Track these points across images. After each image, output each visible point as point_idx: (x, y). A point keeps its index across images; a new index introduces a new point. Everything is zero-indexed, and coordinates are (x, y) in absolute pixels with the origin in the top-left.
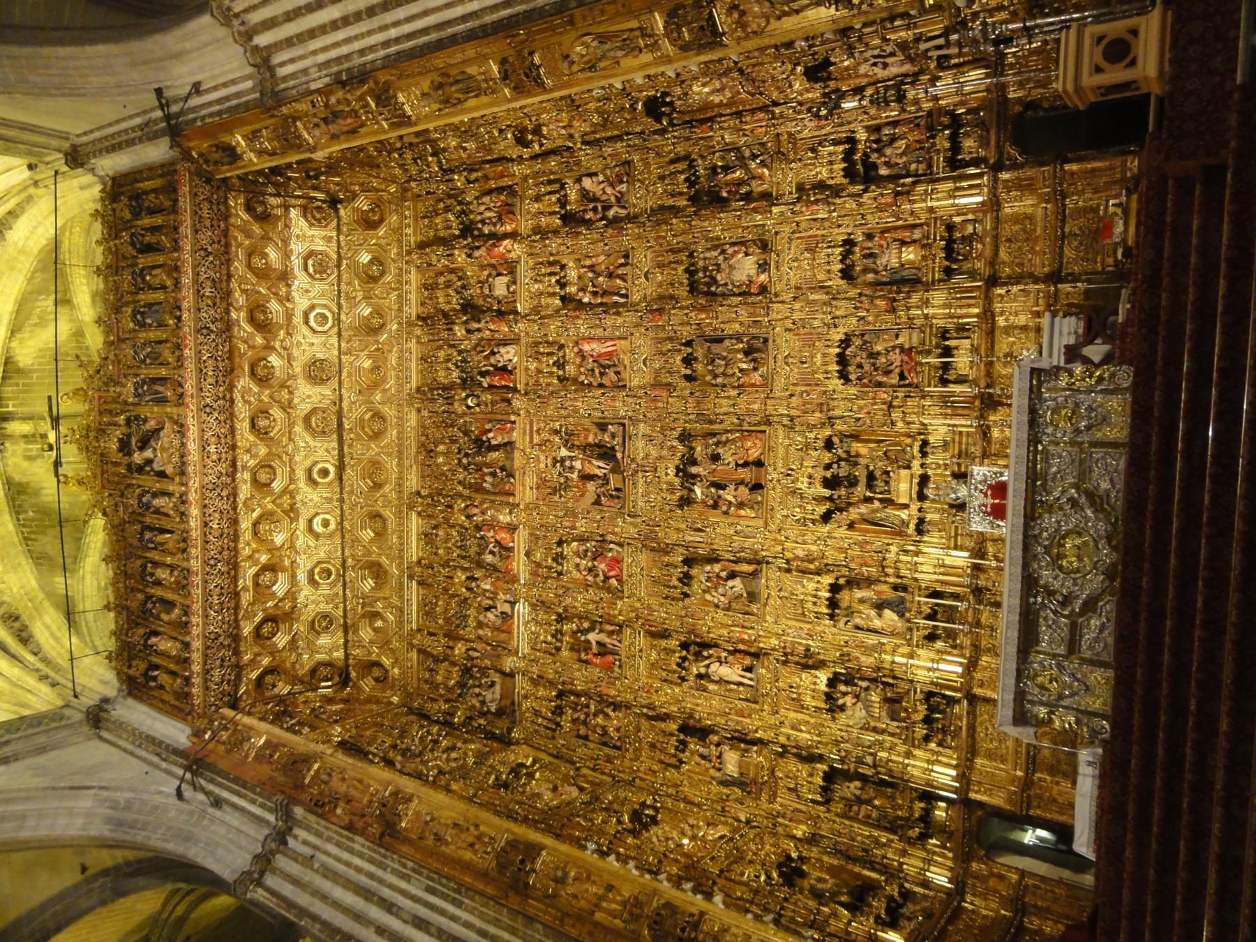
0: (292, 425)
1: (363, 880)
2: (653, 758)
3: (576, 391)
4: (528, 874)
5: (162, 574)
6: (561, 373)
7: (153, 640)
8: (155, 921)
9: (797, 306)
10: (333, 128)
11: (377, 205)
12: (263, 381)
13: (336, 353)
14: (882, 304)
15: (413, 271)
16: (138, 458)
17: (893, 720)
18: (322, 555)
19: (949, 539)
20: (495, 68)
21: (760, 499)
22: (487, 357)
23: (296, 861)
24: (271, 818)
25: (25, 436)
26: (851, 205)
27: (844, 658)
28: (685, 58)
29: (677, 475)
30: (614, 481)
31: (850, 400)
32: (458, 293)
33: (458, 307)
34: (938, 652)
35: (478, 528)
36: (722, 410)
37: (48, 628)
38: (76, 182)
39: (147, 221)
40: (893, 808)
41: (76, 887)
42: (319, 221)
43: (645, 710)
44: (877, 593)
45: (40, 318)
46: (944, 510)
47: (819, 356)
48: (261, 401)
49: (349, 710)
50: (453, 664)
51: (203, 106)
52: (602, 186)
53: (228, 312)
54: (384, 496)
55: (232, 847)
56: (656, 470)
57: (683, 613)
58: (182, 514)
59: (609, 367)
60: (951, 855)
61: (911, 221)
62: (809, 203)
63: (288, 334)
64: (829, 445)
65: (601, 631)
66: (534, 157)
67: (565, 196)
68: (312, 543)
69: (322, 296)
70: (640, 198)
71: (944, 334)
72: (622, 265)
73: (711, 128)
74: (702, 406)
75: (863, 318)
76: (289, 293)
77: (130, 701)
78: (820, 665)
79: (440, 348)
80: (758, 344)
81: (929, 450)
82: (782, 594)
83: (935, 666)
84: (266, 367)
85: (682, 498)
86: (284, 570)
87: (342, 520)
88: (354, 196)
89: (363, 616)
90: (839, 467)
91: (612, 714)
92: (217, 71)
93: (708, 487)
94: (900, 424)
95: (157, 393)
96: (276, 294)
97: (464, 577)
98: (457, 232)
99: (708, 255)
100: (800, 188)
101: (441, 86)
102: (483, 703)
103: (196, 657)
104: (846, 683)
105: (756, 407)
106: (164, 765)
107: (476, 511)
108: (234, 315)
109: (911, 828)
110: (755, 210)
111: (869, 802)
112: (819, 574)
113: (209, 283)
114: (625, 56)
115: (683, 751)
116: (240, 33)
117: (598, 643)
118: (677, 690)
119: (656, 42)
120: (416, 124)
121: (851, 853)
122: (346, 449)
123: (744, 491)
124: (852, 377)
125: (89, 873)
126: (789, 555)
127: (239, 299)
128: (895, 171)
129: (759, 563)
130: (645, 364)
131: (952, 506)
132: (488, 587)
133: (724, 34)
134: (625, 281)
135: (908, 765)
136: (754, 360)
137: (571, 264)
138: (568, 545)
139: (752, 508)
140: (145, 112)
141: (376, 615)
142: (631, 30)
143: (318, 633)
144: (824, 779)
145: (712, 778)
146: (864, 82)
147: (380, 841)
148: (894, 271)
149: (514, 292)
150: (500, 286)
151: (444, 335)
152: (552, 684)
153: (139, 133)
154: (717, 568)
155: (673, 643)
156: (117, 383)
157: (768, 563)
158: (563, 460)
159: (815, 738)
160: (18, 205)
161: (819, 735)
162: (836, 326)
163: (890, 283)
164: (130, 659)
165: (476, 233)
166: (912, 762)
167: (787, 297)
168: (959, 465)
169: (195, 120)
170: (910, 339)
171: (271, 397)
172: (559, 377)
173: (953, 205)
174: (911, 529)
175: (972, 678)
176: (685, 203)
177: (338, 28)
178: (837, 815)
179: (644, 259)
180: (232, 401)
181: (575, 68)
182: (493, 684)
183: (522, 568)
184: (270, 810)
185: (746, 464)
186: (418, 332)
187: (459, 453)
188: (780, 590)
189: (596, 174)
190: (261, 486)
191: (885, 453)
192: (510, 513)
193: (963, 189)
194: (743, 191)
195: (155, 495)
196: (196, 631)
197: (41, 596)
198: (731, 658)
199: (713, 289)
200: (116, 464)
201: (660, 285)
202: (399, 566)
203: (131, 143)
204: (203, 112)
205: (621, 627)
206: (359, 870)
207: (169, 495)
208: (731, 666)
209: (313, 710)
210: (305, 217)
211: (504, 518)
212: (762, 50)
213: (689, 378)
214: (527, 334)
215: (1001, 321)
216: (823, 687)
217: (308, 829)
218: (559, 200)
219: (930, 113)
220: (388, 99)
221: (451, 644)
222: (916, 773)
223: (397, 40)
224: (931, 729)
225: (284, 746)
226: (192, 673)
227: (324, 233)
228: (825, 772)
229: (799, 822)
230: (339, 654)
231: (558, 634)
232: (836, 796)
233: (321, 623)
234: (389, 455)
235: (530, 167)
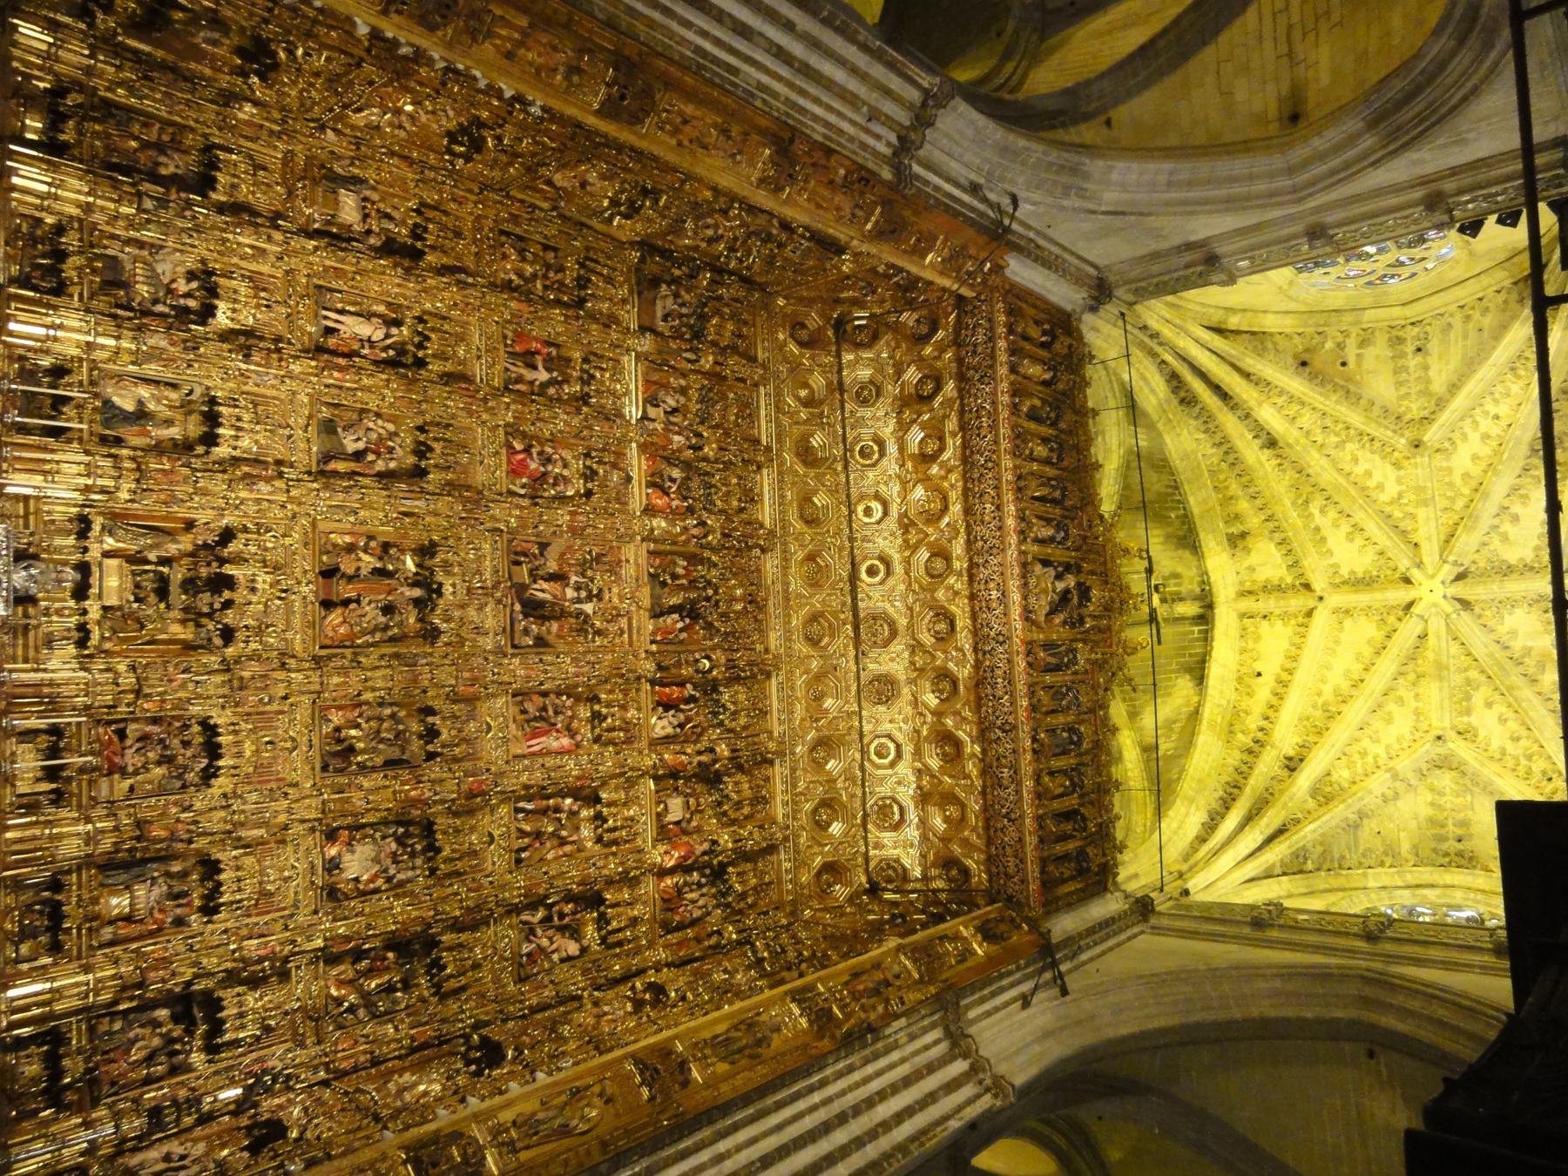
0: (910, 626)
1: (812, 89)
2: (457, 218)
3: (577, 686)
4: (615, 82)
5: (1041, 451)
6: (597, 707)
7: (1047, 376)
8: (1036, 58)
9: (282, 818)
10: (878, 976)
11: (824, 893)
12: (944, 677)
13: (864, 713)
14: (157, 832)
15: (780, 818)
16: (1071, 581)
17: (114, 258)
18: (871, 475)
19: (37, 512)
20: (695, 1074)
21: (325, 558)
22: (689, 720)
23: (887, 116)
24: (916, 168)
25: (1181, 599)
26: (210, 962)
27: (192, 345)
28: (455, 1123)
29: (441, 585)
31: (199, 696)
32: (727, 796)
33: (726, 779)
34: (47, 352)
35: (691, 510)
37: (1152, 391)
38: (1143, 881)
39: (1071, 846)
40: (108, 136)
41: (1117, 102)
42: (889, 867)
43: (470, 280)
44: (146, 434)
45: (1172, 729)
46: (46, 550)
47: (248, 753)
48: (945, 652)
49: (834, 291)
50: (714, 344)
51: (1019, 982)
52: (554, 946)
53: (984, 751)
54: (802, 546)
55: (957, 137)
56: (469, 590)
57: (424, 406)
58: (1023, 519)
59: (536, 719)
60: (15, 64)
61: (118, 950)
62: (272, 957)
63: (917, 732)
64: (228, 635)
65: (532, 383)
66: (641, 972)
67: (599, 929)
68: (883, 489)
69: (882, 779)
70: (503, 937)
71: (58, 798)
72: (524, 850)
73: (413, 1039)
74: (409, 676)
75: (185, 810)
76: (919, 778)
77: (1069, 308)
78: (226, 336)
79: (745, 728)
80: (336, 763)
81: (75, 635)
82: (287, 432)
83: (52, 332)
84: (941, 691)
85: (433, 555)
86: (912, 456)
87: (850, 515)
88: (851, 900)
89: (821, 402)
90: (211, 605)
91: (514, 277)
92: (1006, 1023)
93: (397, 571)
94: (122, 668)
95: (1052, 655)
96: (933, 776)
98: (730, 869)
99: (410, 874)
100: (284, 976)
101: (759, 1043)
102: (676, 295)
103: (1003, 357)
104: (186, 310)
105: (336, 680)
106: (1032, 235)
107: (695, 531)
108: (977, 748)
109: (80, 106)
110: (347, 939)
111: (146, 145)
112: (234, 458)
113: (1005, 782)
114: (534, 1114)
115: (416, 225)
116: (984, 1070)
117: (535, 368)
118: (428, 306)
119: (495, 1138)
120: (786, 993)
121: (171, 76)
122: (849, 601)
123: (347, 566)
124: (196, 728)
125: (1103, 118)
126: (279, 484)
127: (972, 768)
128: (145, 1017)
129: (322, 473)
131: (35, 557)
132: (676, 438)
133: (405, 1162)
134: (519, 830)
135: (88, 194)
136: (339, 741)
137: (589, 844)
138: (577, 492)
139: (335, 545)
140: (1077, 968)
141: (808, 403)
142: (527, 1148)
143: (871, 382)
144: (214, 180)
145: (374, 189)
146: (198, 1132)
147: (795, 133)
148: (141, 879)
149: (658, 803)
150: (676, 809)
151: (740, 744)
152: (593, 317)
153: (1082, 943)
154: (380, 466)
155: (435, 367)
156: (1094, 663)
157: (309, 473)
158: (589, 598)
159: (231, 236)
160: (1197, 851)
161: (225, 241)
162: (225, 795)
163: (145, 861)
164: (1070, 355)
165: (708, 871)
166: (82, 198)
167: (298, 829)
168: (26, 615)
169: (1027, 966)
170: (111, 787)
171: (934, 657)
172: (599, 701)
173: (53, 980)
174: (97, 523)
176: (444, 938)
177: (878, 1093)
178: (192, 130)
179: (496, 860)
180: (976, 650)
181: (597, 1089)
182: (665, 318)
183: (635, 462)
184: (918, 177)
185: (346, 603)
186: (772, 746)
187: (717, 604)
188: (290, 437)
189: (562, 961)
190: (941, 553)
191: (142, 627)
192: (652, 530)
193: (38, 1005)
194: (365, 963)
195: (1052, 539)
196: (1004, 386)
197: (1160, 426)
198: (356, 346)
199: (401, 830)
200: (1092, 573)
201: (473, 829)
202: (782, 464)
203: (1091, 931)
204: (1018, 976)
205: (506, 388)
206: (817, 101)
207: (1037, 541)
208: (355, 337)
209: (874, 292)
210: (905, 869)
211: (660, 524)
212: (349, 1151)
213: (430, 711)
214: (640, 753)
216: (222, 306)
217: (876, 153)
218: (608, 923)
219: (95, 1103)
220: (819, 1018)
221: (718, 368)
222: (75, 183)
223: (811, 1090)
224: (54, 243)
225: (905, 251)
226: (1006, 338)
227: (884, 852)
228: (214, 189)
229: (248, 123)
230: (848, 357)
231: (587, 379)
232: (194, 156)
233: (868, 394)
234: (800, 596)
235: (645, 960)
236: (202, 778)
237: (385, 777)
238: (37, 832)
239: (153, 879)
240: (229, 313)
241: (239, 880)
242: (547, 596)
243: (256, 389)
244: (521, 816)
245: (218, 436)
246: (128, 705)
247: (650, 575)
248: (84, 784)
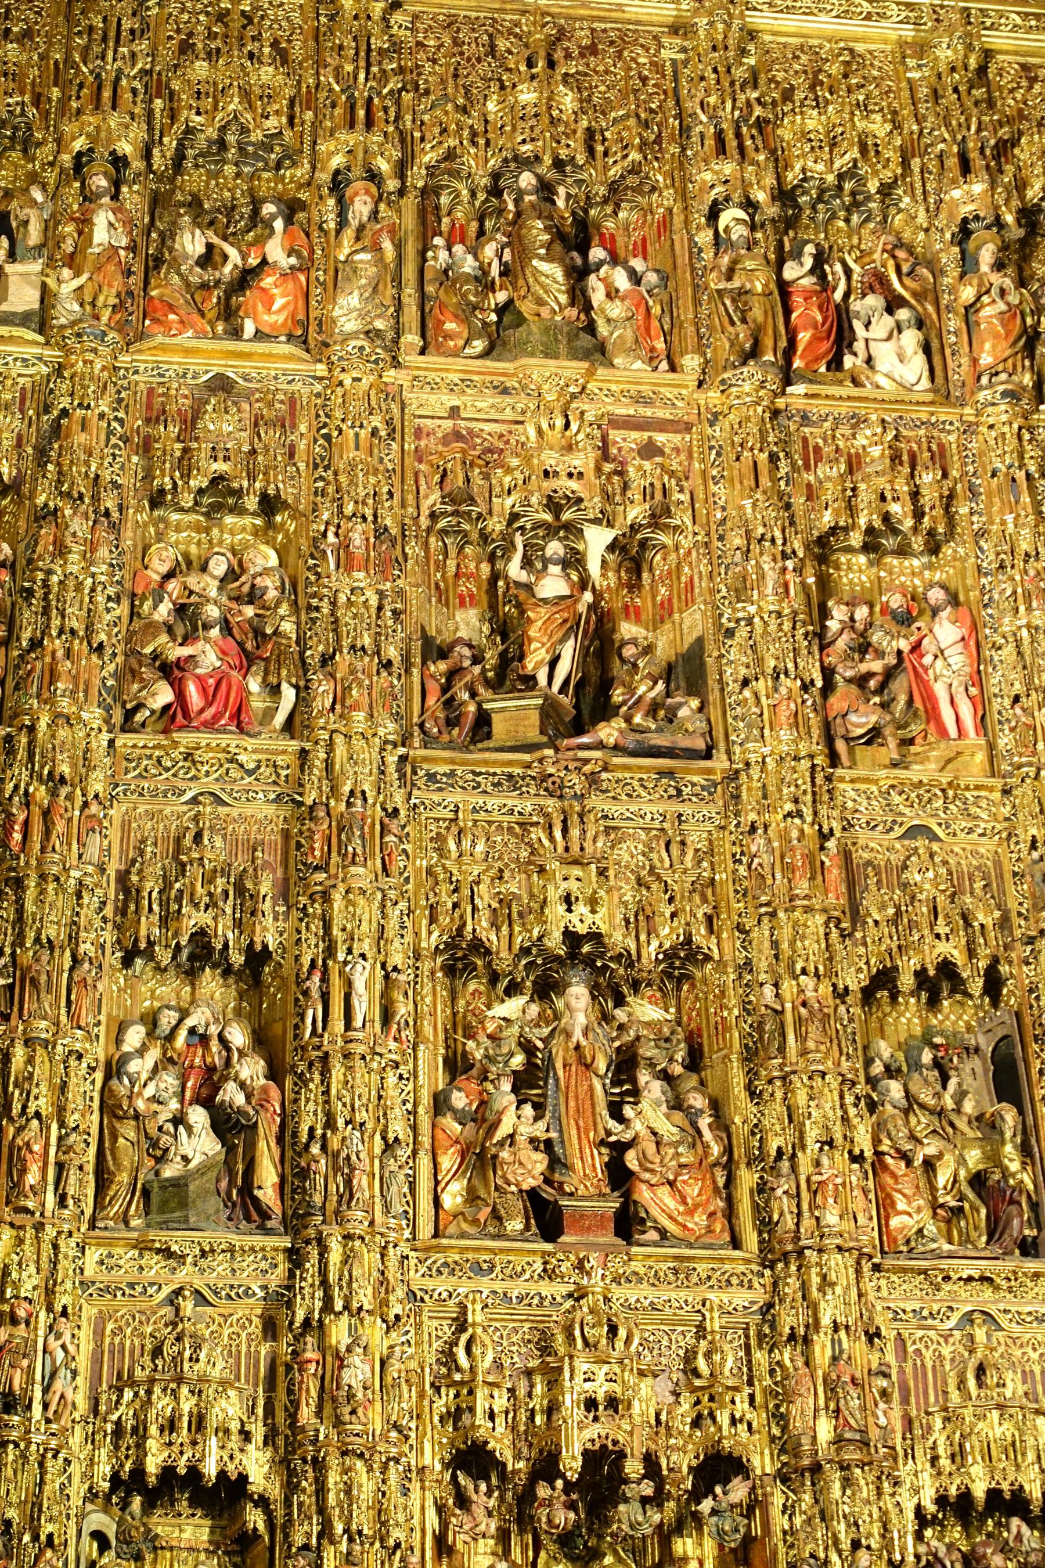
6: (856, 539)
22: (878, 282)
36: (801, 1097)
57: (86, 948)
82: (188, 1307)
85: (478, 946)
93: (528, 1048)
97: (125, 148)
126: (339, 1333)
132: (101, 235)
139: (472, 1197)
186: (945, 54)
187: (558, 164)
242: (568, 652)
245: (222, 1474)
247: (486, 354)
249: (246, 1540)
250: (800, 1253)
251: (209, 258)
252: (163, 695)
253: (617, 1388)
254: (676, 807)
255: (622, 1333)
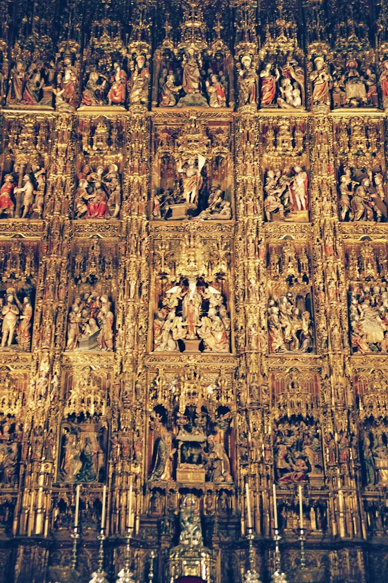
30: (179, 209)
34: (51, 512)
47: (299, 400)
59: (282, 202)
64: (223, 410)
71: (321, 507)
72: (375, 213)
75: (332, 437)
81: (224, 494)
83: (39, 511)
94: (244, 472)
97: (74, 49)
104: (12, 429)
112: (108, 404)
130: (285, 238)
132: (67, 77)
134: (362, 217)
148: (373, 463)
162: (324, 413)
163: (361, 458)
175: (31, 544)
199: (355, 301)
201: (358, 252)
211: (135, 95)
215: (333, 555)
236: (312, 425)
237: (318, 311)
238: (341, 520)
239: (373, 455)
240: (13, 406)
241: (379, 407)
243: (62, 390)
244: (351, 216)
245: (95, 414)
246: (267, 469)
248: (314, 492)
249: (103, 429)
250: (245, 354)
251: (99, 81)
252: (85, 208)
253: (196, 390)
254: (221, 234)
255: (198, 376)
